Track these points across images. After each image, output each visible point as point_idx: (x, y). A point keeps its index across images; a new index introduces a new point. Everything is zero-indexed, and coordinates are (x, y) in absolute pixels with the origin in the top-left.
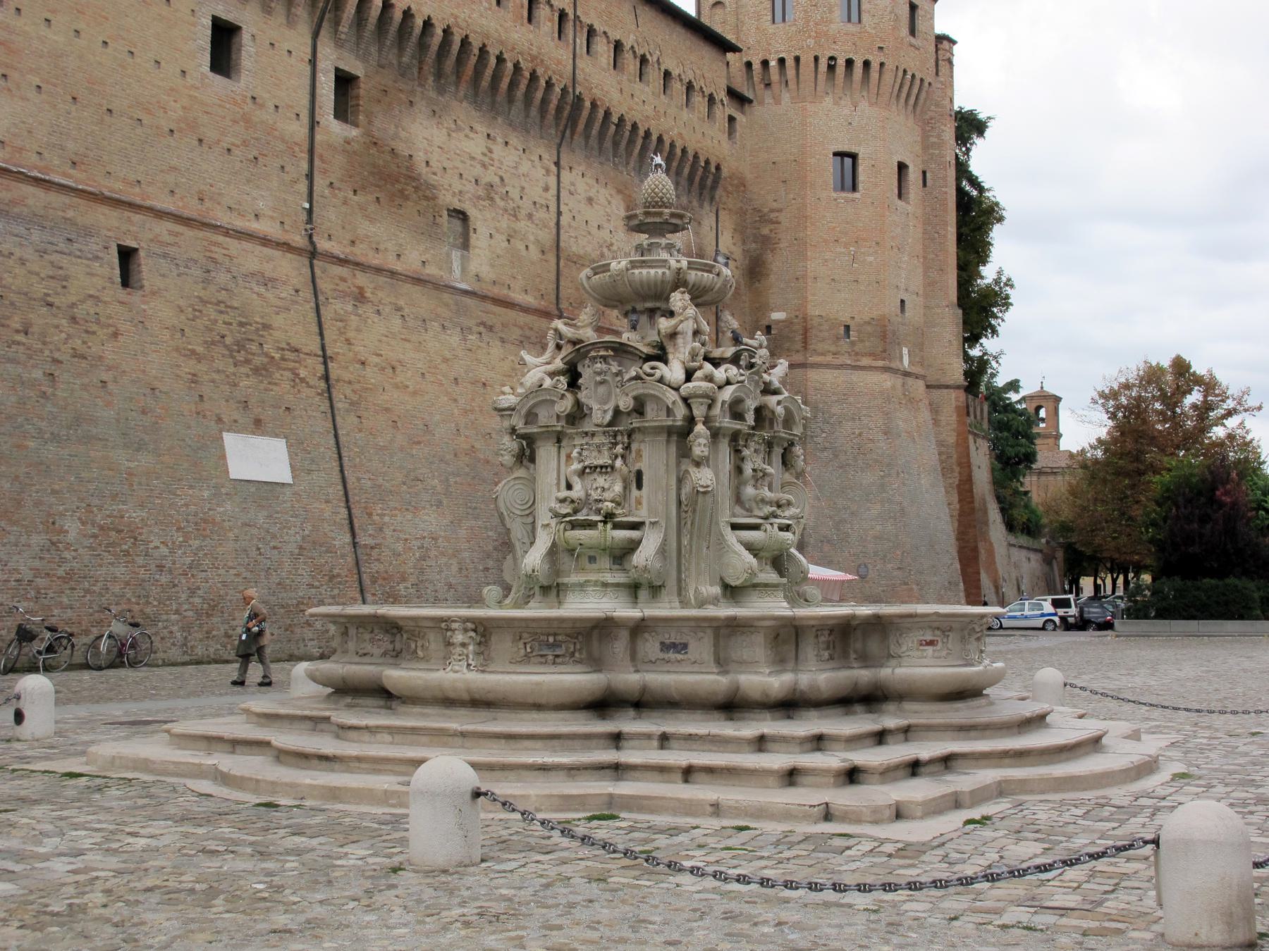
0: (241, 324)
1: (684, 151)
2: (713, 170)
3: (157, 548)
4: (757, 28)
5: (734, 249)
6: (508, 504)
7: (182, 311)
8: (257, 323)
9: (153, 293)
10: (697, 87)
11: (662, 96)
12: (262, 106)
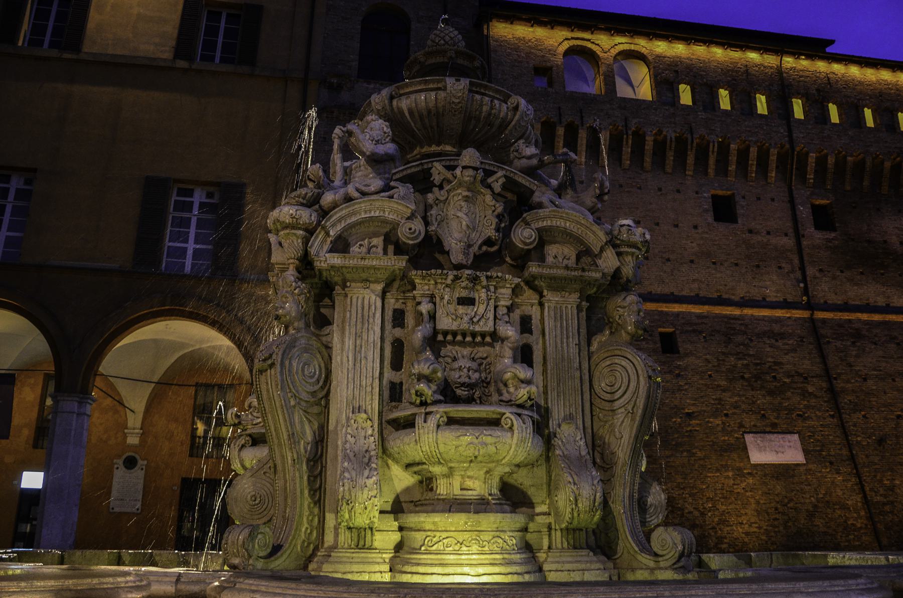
0: (757, 364)
3: (690, 513)
7: (709, 362)
8: (768, 362)
9: (687, 355)
12: (758, 233)
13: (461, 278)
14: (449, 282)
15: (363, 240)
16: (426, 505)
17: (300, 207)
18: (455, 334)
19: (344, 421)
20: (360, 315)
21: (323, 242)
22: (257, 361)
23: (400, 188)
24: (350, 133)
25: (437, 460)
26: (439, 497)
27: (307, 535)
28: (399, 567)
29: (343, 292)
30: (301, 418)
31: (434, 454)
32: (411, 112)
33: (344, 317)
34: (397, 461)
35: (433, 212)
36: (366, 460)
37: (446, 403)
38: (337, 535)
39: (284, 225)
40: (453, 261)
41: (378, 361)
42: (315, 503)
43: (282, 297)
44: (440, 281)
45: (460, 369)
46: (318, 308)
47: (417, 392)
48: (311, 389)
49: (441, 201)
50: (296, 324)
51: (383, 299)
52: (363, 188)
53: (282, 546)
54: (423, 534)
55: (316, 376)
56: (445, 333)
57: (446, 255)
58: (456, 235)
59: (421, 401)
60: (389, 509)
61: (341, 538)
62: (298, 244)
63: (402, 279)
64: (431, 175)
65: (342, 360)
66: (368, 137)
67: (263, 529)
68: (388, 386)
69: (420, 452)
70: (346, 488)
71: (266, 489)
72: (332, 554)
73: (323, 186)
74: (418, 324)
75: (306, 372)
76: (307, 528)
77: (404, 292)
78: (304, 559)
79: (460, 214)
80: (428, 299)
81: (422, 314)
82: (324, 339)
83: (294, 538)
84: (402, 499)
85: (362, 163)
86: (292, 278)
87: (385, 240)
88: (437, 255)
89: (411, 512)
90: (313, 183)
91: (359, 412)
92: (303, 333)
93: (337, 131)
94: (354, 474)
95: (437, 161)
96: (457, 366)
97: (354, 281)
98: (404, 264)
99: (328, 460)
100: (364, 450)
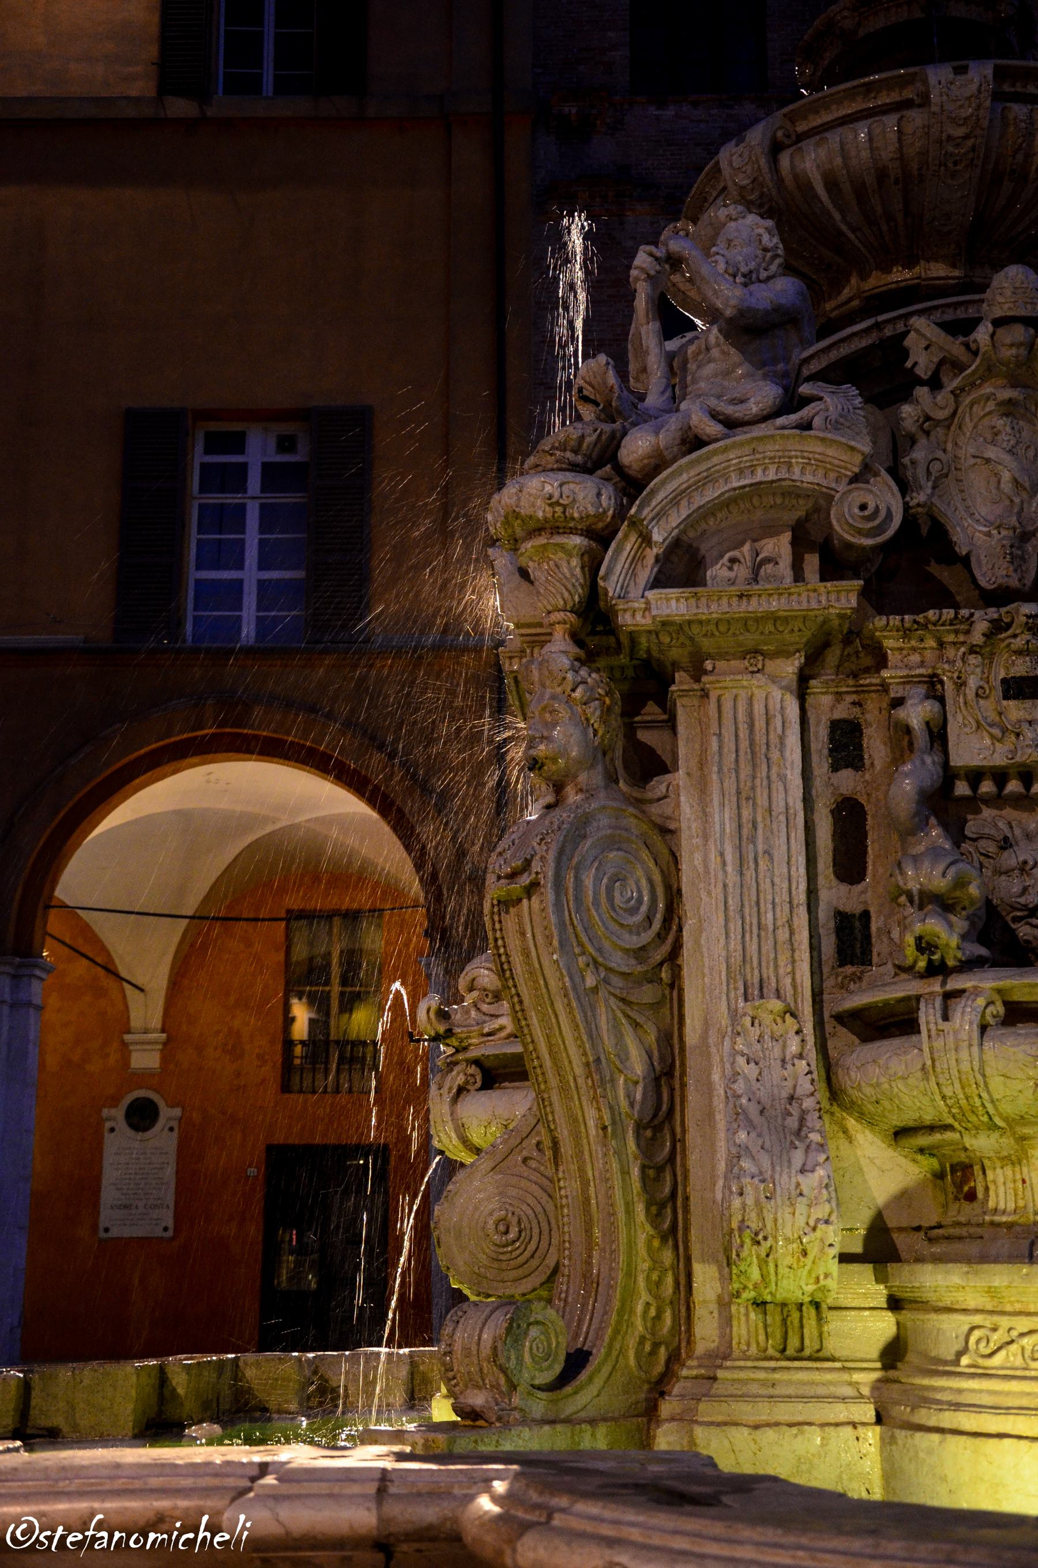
13: (1009, 626)
14: (977, 637)
15: (739, 545)
16: (960, 1238)
17: (569, 476)
18: (1000, 777)
19: (725, 1021)
20: (744, 744)
21: (637, 559)
22: (494, 878)
23: (827, 399)
24: (675, 262)
25: (985, 1119)
26: (997, 1218)
27: (649, 1325)
28: (901, 1411)
29: (696, 686)
30: (615, 1018)
31: (977, 1102)
32: (831, 183)
33: (704, 750)
34: (869, 1121)
35: (919, 454)
36: (792, 1123)
37: (995, 964)
38: (727, 1321)
39: (532, 525)
40: (983, 583)
41: (802, 860)
42: (664, 1239)
43: (544, 709)
44: (951, 638)
45: (1022, 870)
46: (630, 731)
47: (919, 939)
48: (635, 941)
49: (937, 423)
50: (583, 778)
51: (802, 698)
52: (730, 410)
53: (589, 1353)
54: (964, 1321)
55: (644, 908)
56: (975, 776)
57: (959, 567)
58: (984, 510)
59: (930, 962)
60: (858, 1248)
61: (740, 1331)
62: (571, 569)
63: (847, 641)
64: (905, 354)
65: (705, 861)
66: (721, 267)
67: (539, 1311)
68: (832, 924)
69: (938, 1098)
70: (750, 1201)
71: (530, 1200)
72: (720, 1374)
73: (619, 413)
74: (898, 758)
75: (618, 900)
76: (648, 1304)
77: (855, 676)
78: (646, 1387)
79: (991, 453)
80: (922, 690)
81: (908, 730)
82: (654, 810)
83: (617, 1332)
84: (891, 1223)
85: (712, 339)
86: (565, 662)
87: (795, 543)
88: (935, 569)
89: (920, 1260)
90: (591, 407)
91: (762, 997)
92: (602, 799)
93: (642, 259)
94: (765, 1161)
95: (920, 313)
96: (1013, 862)
97: (723, 656)
98: (854, 603)
99: (690, 1123)
100: (784, 1094)
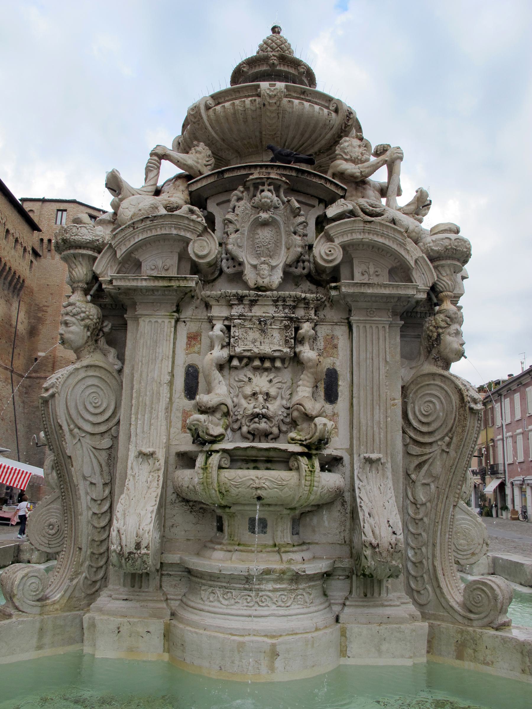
1: (10, 268)
2: (21, 281)
4: (48, 225)
5: (24, 320)
6: (73, 412)
10: (20, 242)
11: (4, 240)
